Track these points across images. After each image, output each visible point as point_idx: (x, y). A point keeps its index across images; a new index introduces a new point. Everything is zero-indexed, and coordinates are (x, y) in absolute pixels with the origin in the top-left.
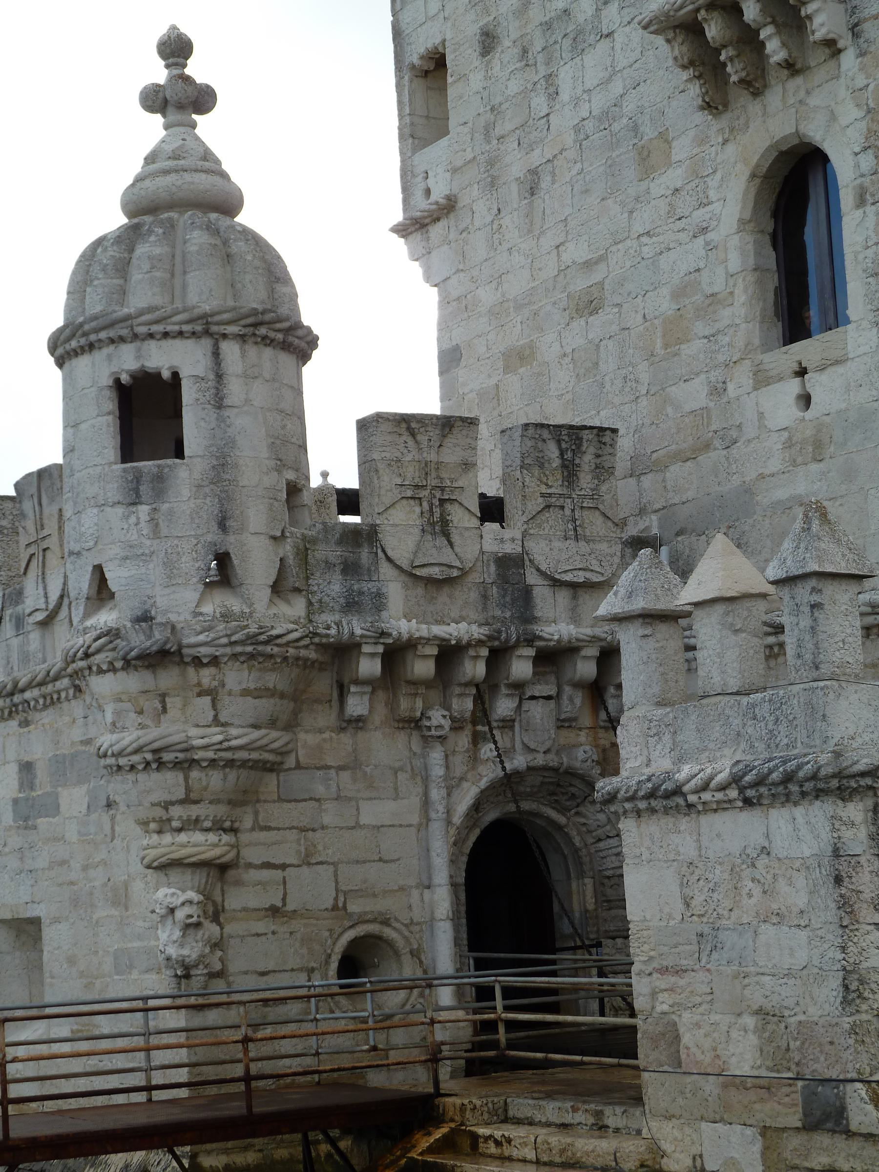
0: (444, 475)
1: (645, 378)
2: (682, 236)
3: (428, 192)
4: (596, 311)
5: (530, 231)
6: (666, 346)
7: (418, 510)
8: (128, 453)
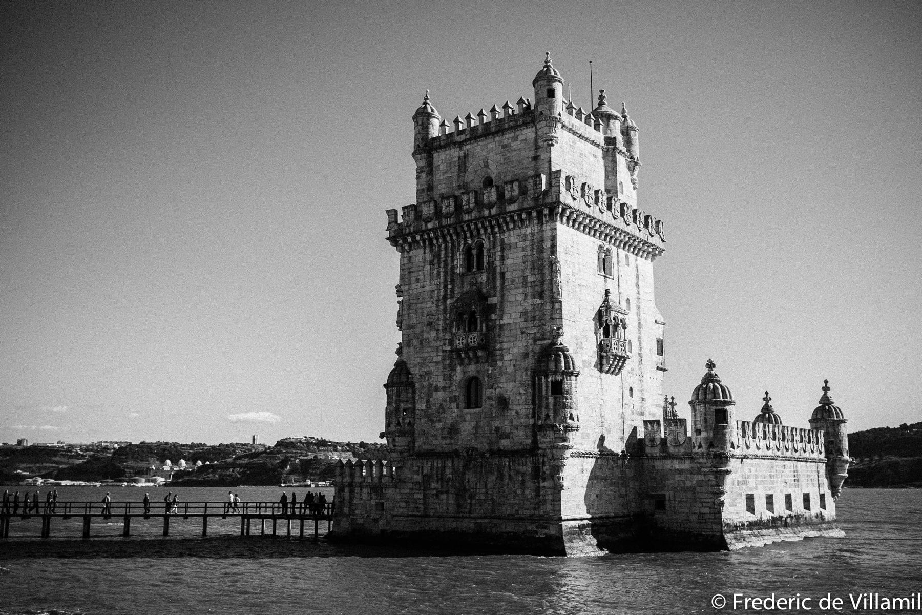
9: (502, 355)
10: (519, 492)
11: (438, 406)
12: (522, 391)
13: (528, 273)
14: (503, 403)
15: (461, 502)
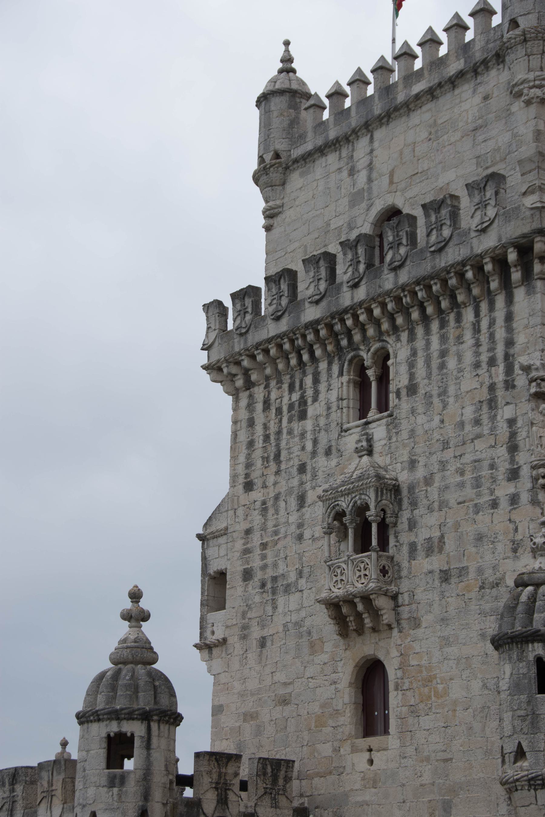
0: (227, 778)
1: (306, 738)
2: (326, 682)
3: (213, 633)
4: (287, 704)
5: (260, 663)
6: (316, 727)
7: (216, 793)
8: (109, 766)
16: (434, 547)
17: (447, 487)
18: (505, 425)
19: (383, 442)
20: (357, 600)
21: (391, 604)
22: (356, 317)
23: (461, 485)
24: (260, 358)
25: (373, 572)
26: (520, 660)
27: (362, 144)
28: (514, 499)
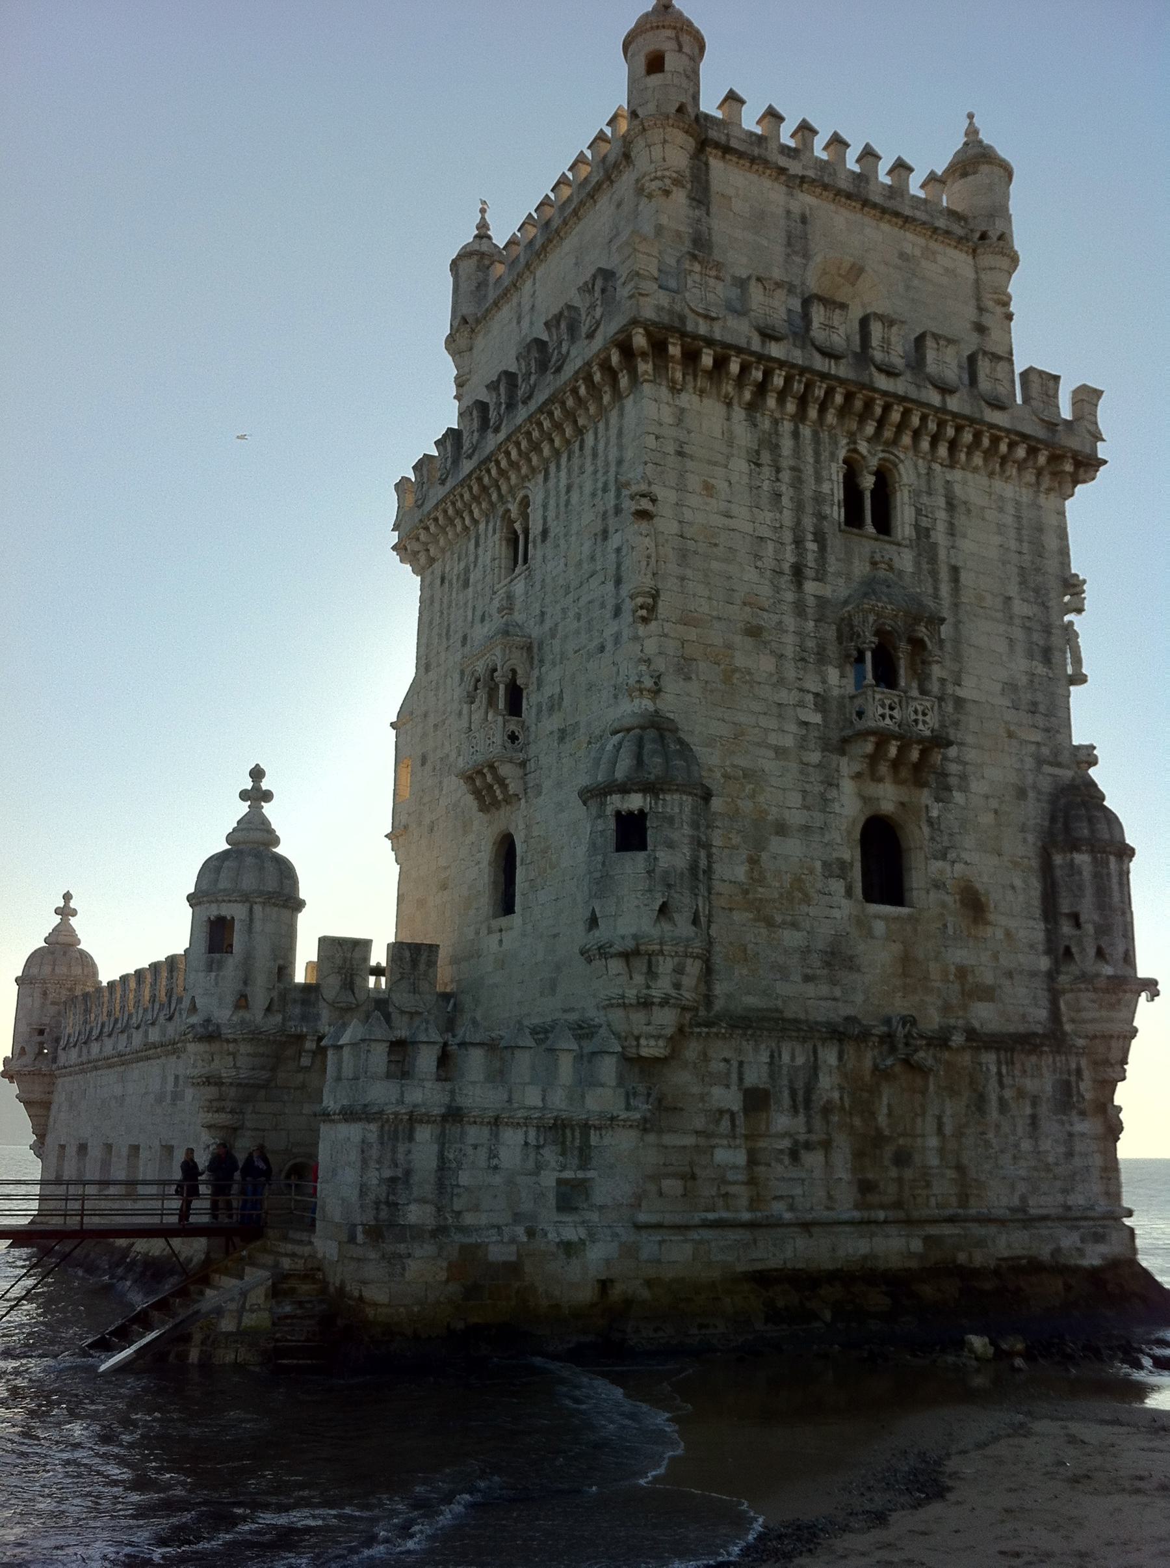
8: (211, 950)
9: (963, 777)
10: (1026, 1145)
11: (788, 878)
12: (1018, 883)
13: (1013, 590)
14: (974, 904)
15: (870, 1176)
16: (555, 704)
17: (566, 637)
18: (614, 556)
19: (523, 598)
20: (485, 771)
21: (520, 772)
22: (498, 463)
23: (577, 632)
24: (433, 529)
25: (499, 738)
26: (599, 817)
27: (527, 287)
28: (617, 638)
